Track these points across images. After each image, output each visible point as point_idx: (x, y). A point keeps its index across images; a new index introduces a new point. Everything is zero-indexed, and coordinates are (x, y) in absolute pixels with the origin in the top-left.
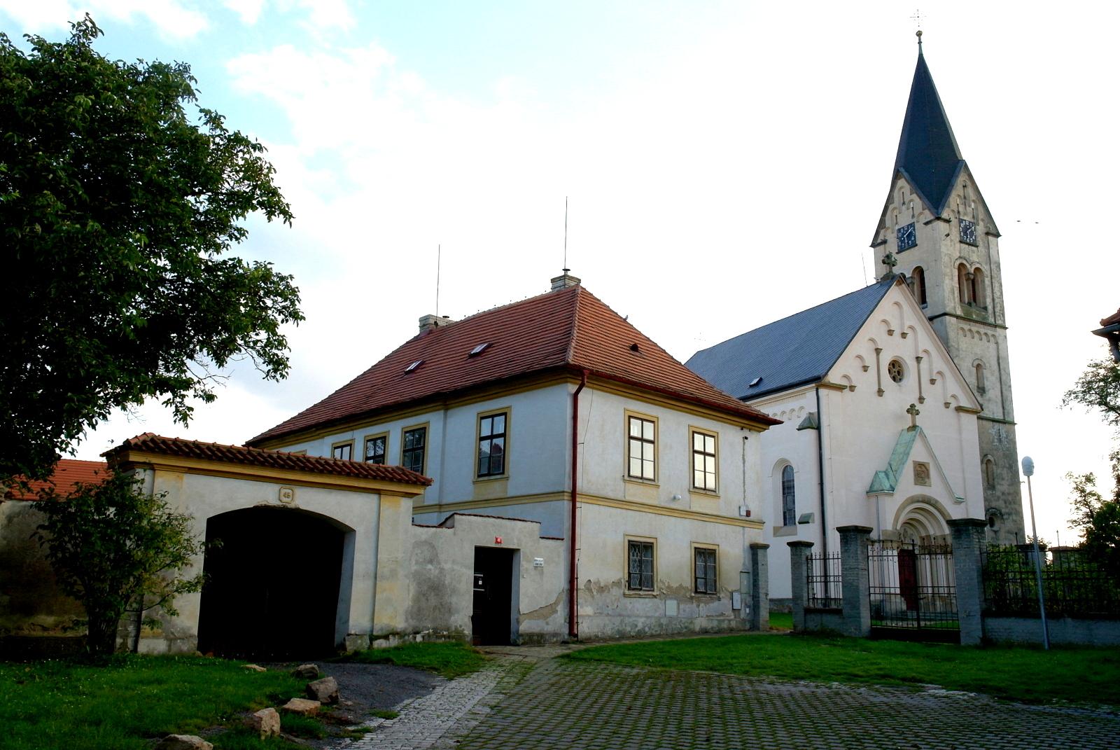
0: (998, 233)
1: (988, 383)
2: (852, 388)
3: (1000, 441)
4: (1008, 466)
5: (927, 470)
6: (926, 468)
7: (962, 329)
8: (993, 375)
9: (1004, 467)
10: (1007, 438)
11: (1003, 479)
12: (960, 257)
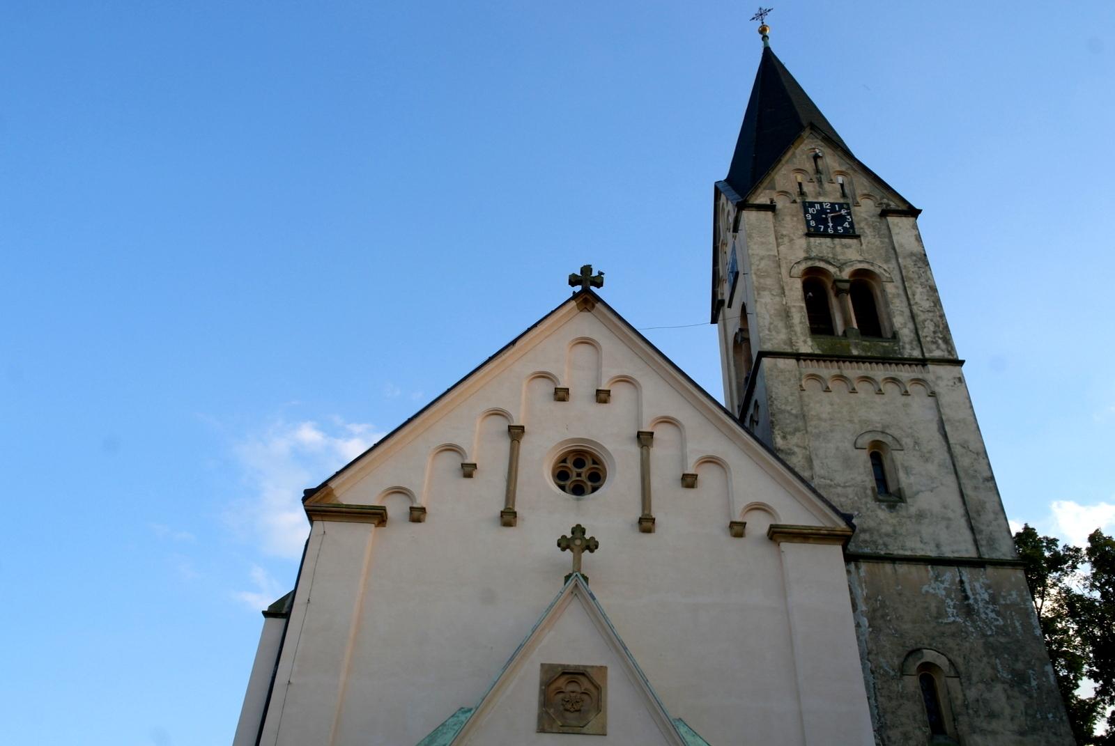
0: (911, 207)
1: (912, 479)
2: (417, 514)
3: (969, 611)
4: (1007, 676)
5: (598, 688)
7: (814, 377)
8: (926, 458)
9: (995, 679)
10: (993, 600)
11: (992, 715)
12: (806, 259)
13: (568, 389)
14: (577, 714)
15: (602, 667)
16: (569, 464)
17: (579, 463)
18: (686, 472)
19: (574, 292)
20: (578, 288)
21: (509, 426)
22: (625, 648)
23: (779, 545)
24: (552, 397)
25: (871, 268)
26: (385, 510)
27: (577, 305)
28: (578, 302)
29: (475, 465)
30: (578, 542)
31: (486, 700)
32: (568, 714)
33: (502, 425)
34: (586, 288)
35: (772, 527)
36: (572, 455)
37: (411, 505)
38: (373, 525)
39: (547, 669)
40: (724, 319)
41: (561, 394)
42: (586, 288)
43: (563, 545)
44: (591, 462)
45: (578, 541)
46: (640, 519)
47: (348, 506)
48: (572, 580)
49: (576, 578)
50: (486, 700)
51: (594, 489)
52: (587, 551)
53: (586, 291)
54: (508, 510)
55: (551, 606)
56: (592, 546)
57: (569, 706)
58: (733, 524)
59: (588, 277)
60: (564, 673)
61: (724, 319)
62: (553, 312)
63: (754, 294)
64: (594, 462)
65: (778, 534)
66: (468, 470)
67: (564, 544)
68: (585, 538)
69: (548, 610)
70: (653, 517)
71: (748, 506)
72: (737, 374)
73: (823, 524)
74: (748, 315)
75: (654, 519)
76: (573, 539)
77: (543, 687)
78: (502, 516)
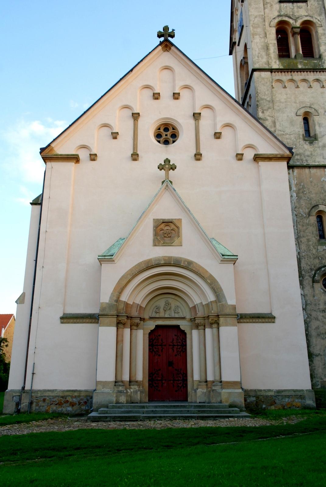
2: (93, 157)
5: (178, 227)
6: (175, 225)
7: (279, 81)
12: (279, 16)
13: (159, 93)
14: (170, 238)
15: (179, 219)
16: (162, 130)
17: (166, 130)
18: (216, 131)
19: (160, 41)
20: (162, 39)
21: (132, 113)
22: (189, 211)
23: (258, 163)
24: (152, 98)
25: (311, 19)
26: (78, 156)
27: (162, 48)
28: (163, 46)
29: (118, 133)
30: (167, 166)
31: (131, 234)
32: (165, 238)
33: (129, 113)
34: (166, 38)
35: (255, 155)
36: (162, 126)
37: (90, 153)
38: (74, 163)
39: (156, 221)
40: (236, 52)
41: (156, 96)
42: (166, 38)
43: (160, 168)
44: (172, 129)
45: (167, 166)
46: (195, 154)
47: (61, 155)
48: (165, 183)
49: (167, 182)
50: (131, 234)
51: (174, 142)
52: (171, 170)
53: (166, 40)
54: (134, 153)
55: (156, 195)
56: (173, 168)
57: (166, 235)
58: (237, 154)
59: (167, 33)
60: (163, 222)
61: (236, 52)
62: (150, 53)
63: (251, 37)
64: (173, 129)
65: (258, 158)
66: (115, 136)
67: (161, 167)
68: (170, 164)
69: (155, 197)
70: (201, 153)
71: (245, 146)
72: (241, 81)
73: (279, 152)
74: (248, 50)
75: (202, 154)
76: (165, 165)
77: (155, 228)
78: (132, 156)
